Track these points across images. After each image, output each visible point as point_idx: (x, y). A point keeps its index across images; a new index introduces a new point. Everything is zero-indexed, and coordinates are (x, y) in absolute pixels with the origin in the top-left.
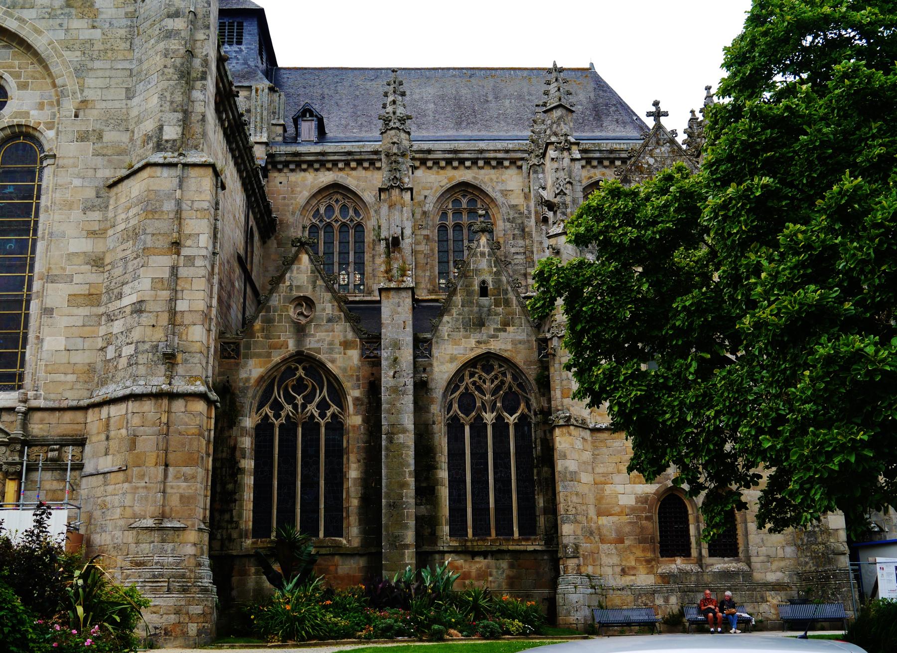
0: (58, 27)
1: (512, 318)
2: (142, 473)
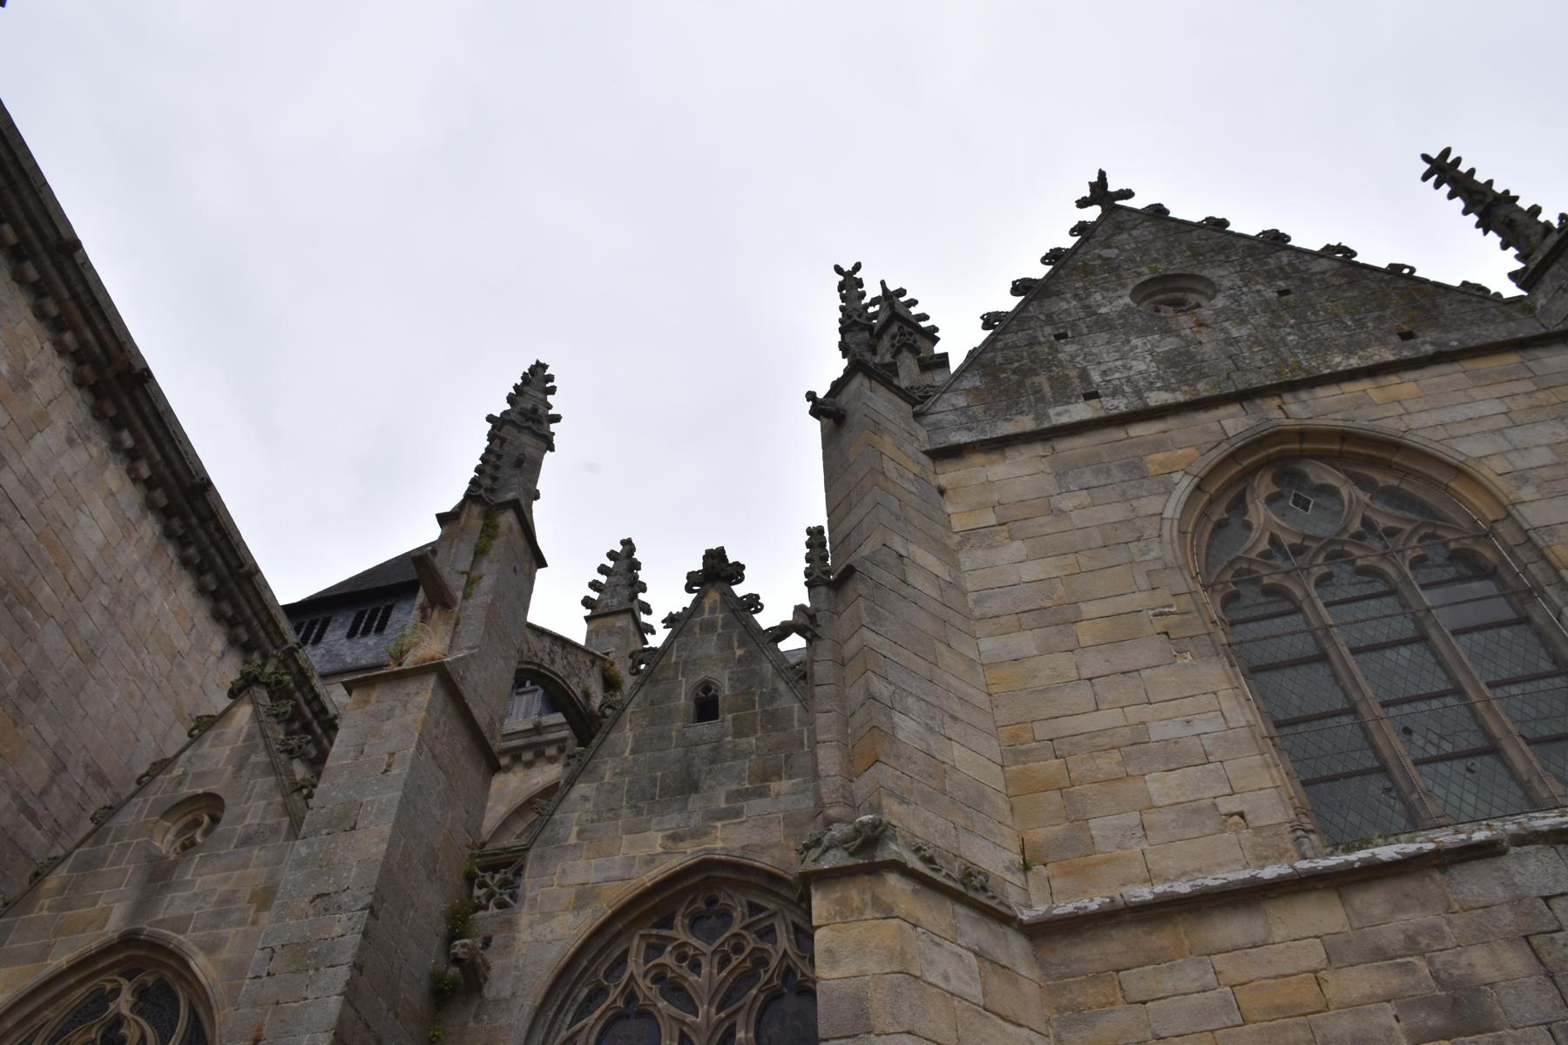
1: (788, 757)
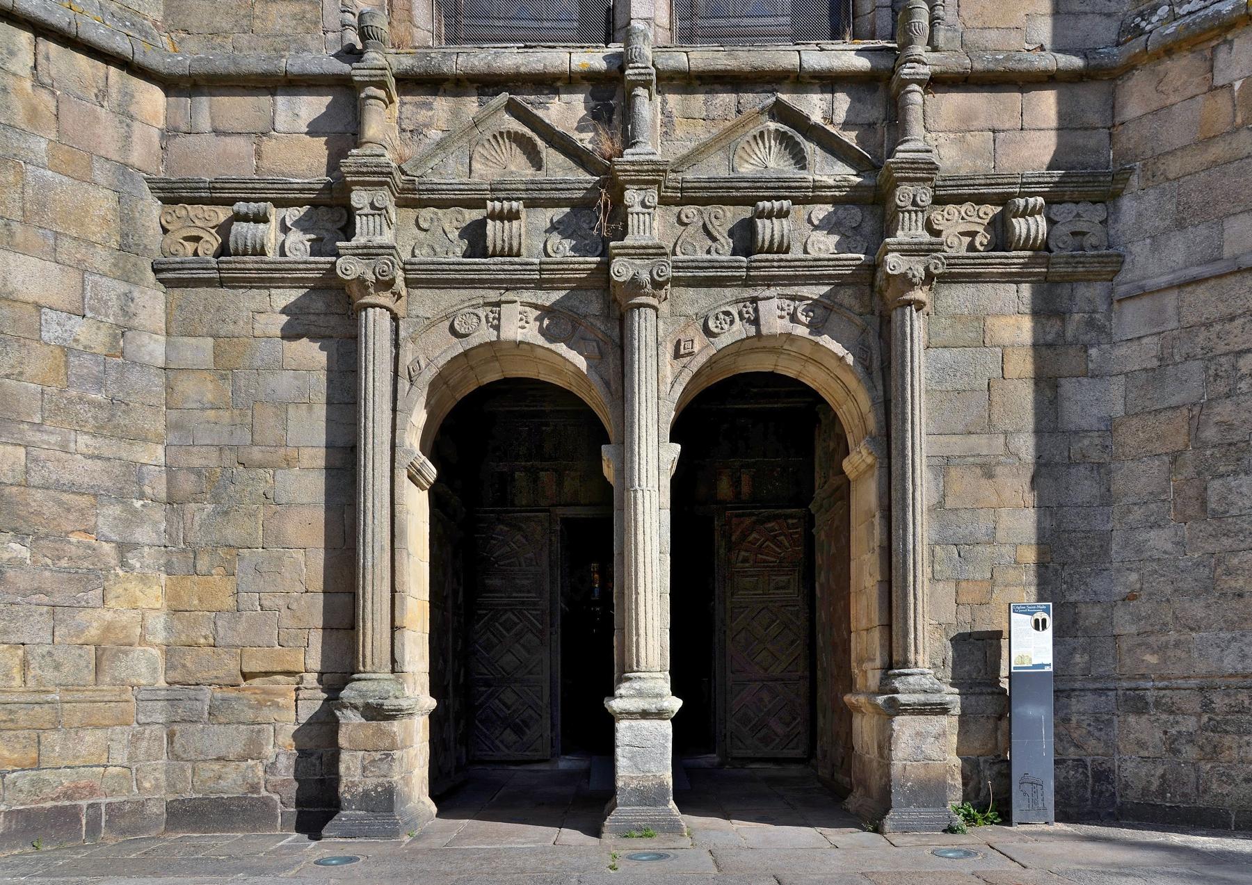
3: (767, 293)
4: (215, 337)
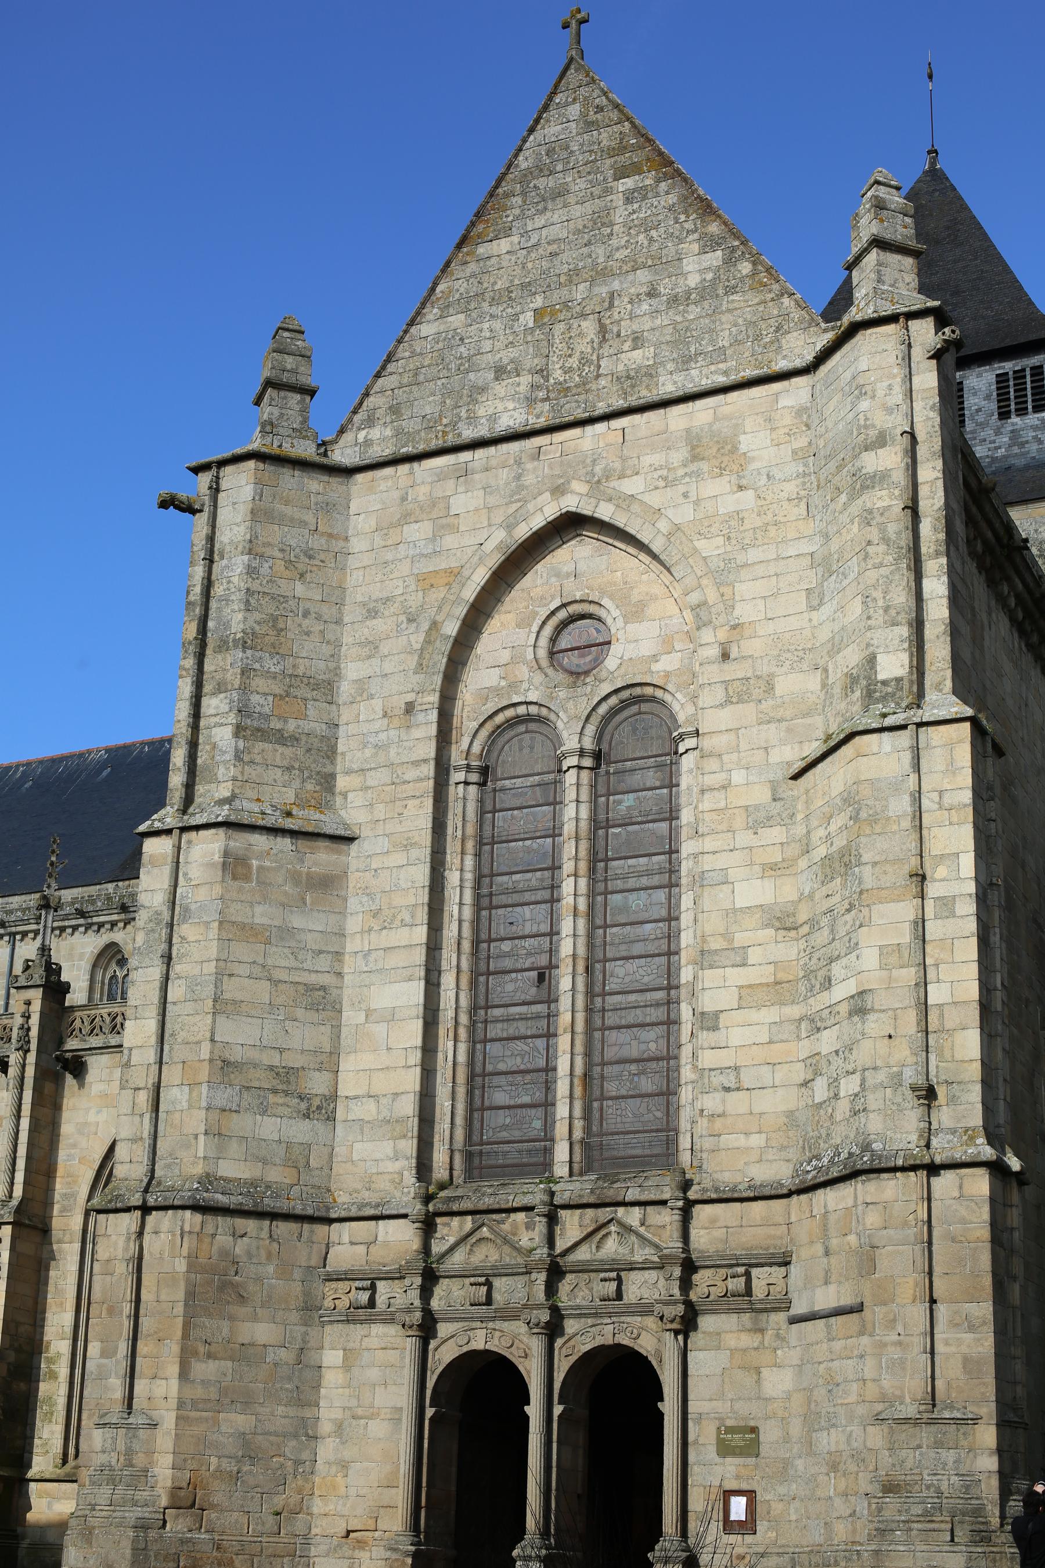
0: (681, 500)
2: (891, 1317)
3: (608, 1321)
4: (344, 1350)
